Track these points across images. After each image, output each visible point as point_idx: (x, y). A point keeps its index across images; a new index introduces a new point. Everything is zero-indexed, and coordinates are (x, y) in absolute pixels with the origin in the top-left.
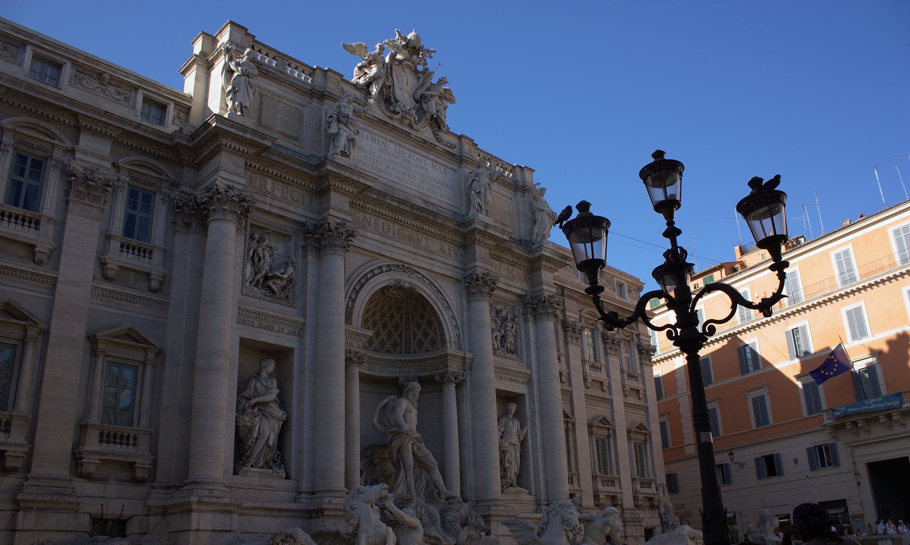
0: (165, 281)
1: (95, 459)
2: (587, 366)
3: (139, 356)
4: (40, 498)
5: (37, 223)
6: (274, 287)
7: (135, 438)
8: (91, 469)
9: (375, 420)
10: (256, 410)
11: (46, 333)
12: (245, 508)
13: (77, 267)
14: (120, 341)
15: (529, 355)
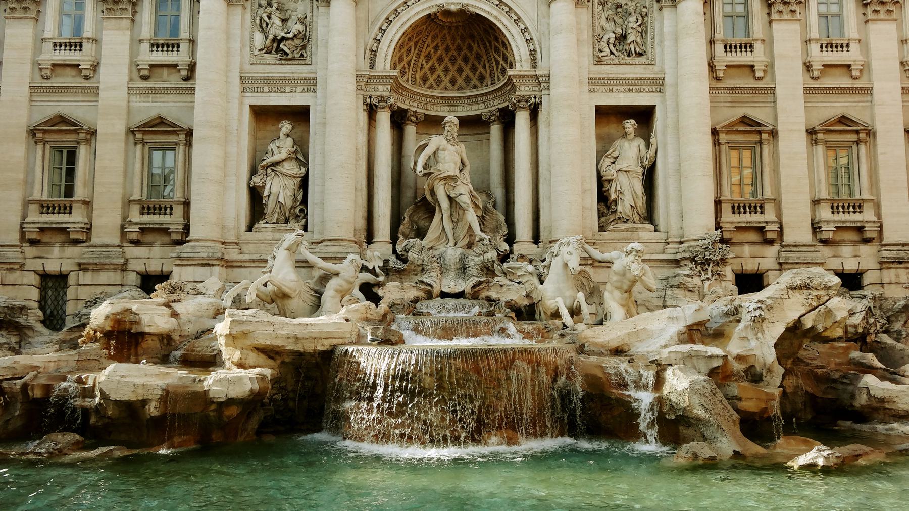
0: (192, 68)
1: (136, 228)
2: (815, 48)
3: (172, 139)
4: (91, 261)
5: (81, 46)
6: (286, 49)
7: (171, 209)
8: (134, 236)
9: (412, 165)
10: (269, 171)
11: (93, 133)
12: (245, 261)
13: (114, 77)
14: (153, 129)
15: (662, 54)
